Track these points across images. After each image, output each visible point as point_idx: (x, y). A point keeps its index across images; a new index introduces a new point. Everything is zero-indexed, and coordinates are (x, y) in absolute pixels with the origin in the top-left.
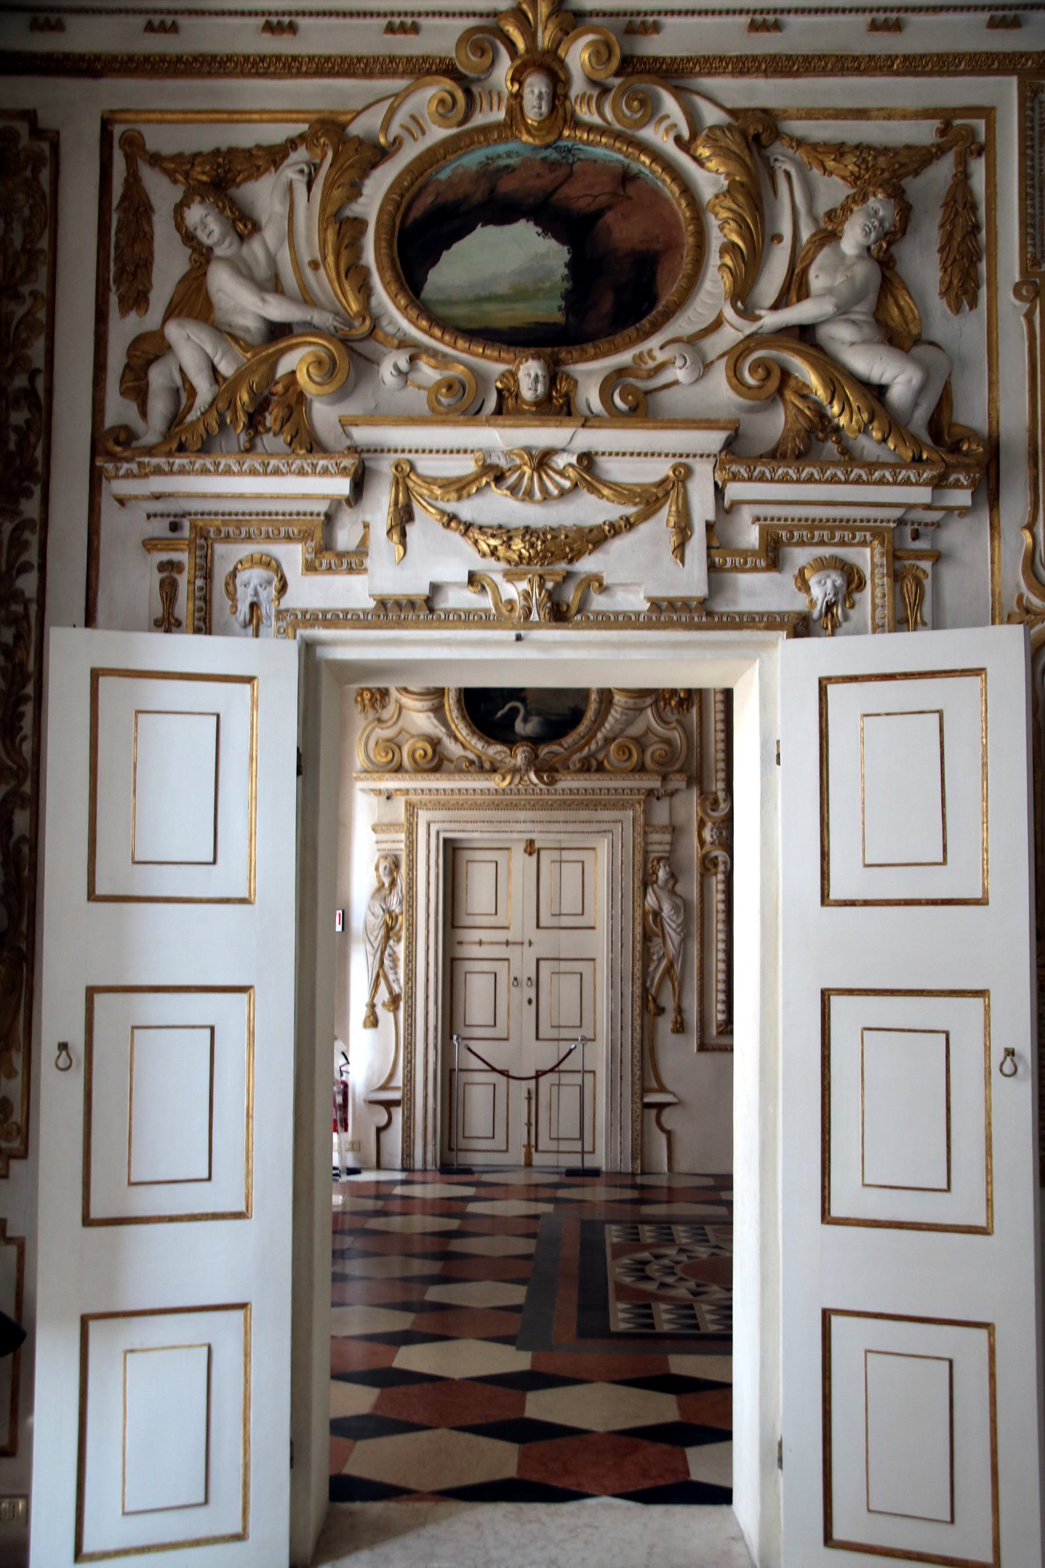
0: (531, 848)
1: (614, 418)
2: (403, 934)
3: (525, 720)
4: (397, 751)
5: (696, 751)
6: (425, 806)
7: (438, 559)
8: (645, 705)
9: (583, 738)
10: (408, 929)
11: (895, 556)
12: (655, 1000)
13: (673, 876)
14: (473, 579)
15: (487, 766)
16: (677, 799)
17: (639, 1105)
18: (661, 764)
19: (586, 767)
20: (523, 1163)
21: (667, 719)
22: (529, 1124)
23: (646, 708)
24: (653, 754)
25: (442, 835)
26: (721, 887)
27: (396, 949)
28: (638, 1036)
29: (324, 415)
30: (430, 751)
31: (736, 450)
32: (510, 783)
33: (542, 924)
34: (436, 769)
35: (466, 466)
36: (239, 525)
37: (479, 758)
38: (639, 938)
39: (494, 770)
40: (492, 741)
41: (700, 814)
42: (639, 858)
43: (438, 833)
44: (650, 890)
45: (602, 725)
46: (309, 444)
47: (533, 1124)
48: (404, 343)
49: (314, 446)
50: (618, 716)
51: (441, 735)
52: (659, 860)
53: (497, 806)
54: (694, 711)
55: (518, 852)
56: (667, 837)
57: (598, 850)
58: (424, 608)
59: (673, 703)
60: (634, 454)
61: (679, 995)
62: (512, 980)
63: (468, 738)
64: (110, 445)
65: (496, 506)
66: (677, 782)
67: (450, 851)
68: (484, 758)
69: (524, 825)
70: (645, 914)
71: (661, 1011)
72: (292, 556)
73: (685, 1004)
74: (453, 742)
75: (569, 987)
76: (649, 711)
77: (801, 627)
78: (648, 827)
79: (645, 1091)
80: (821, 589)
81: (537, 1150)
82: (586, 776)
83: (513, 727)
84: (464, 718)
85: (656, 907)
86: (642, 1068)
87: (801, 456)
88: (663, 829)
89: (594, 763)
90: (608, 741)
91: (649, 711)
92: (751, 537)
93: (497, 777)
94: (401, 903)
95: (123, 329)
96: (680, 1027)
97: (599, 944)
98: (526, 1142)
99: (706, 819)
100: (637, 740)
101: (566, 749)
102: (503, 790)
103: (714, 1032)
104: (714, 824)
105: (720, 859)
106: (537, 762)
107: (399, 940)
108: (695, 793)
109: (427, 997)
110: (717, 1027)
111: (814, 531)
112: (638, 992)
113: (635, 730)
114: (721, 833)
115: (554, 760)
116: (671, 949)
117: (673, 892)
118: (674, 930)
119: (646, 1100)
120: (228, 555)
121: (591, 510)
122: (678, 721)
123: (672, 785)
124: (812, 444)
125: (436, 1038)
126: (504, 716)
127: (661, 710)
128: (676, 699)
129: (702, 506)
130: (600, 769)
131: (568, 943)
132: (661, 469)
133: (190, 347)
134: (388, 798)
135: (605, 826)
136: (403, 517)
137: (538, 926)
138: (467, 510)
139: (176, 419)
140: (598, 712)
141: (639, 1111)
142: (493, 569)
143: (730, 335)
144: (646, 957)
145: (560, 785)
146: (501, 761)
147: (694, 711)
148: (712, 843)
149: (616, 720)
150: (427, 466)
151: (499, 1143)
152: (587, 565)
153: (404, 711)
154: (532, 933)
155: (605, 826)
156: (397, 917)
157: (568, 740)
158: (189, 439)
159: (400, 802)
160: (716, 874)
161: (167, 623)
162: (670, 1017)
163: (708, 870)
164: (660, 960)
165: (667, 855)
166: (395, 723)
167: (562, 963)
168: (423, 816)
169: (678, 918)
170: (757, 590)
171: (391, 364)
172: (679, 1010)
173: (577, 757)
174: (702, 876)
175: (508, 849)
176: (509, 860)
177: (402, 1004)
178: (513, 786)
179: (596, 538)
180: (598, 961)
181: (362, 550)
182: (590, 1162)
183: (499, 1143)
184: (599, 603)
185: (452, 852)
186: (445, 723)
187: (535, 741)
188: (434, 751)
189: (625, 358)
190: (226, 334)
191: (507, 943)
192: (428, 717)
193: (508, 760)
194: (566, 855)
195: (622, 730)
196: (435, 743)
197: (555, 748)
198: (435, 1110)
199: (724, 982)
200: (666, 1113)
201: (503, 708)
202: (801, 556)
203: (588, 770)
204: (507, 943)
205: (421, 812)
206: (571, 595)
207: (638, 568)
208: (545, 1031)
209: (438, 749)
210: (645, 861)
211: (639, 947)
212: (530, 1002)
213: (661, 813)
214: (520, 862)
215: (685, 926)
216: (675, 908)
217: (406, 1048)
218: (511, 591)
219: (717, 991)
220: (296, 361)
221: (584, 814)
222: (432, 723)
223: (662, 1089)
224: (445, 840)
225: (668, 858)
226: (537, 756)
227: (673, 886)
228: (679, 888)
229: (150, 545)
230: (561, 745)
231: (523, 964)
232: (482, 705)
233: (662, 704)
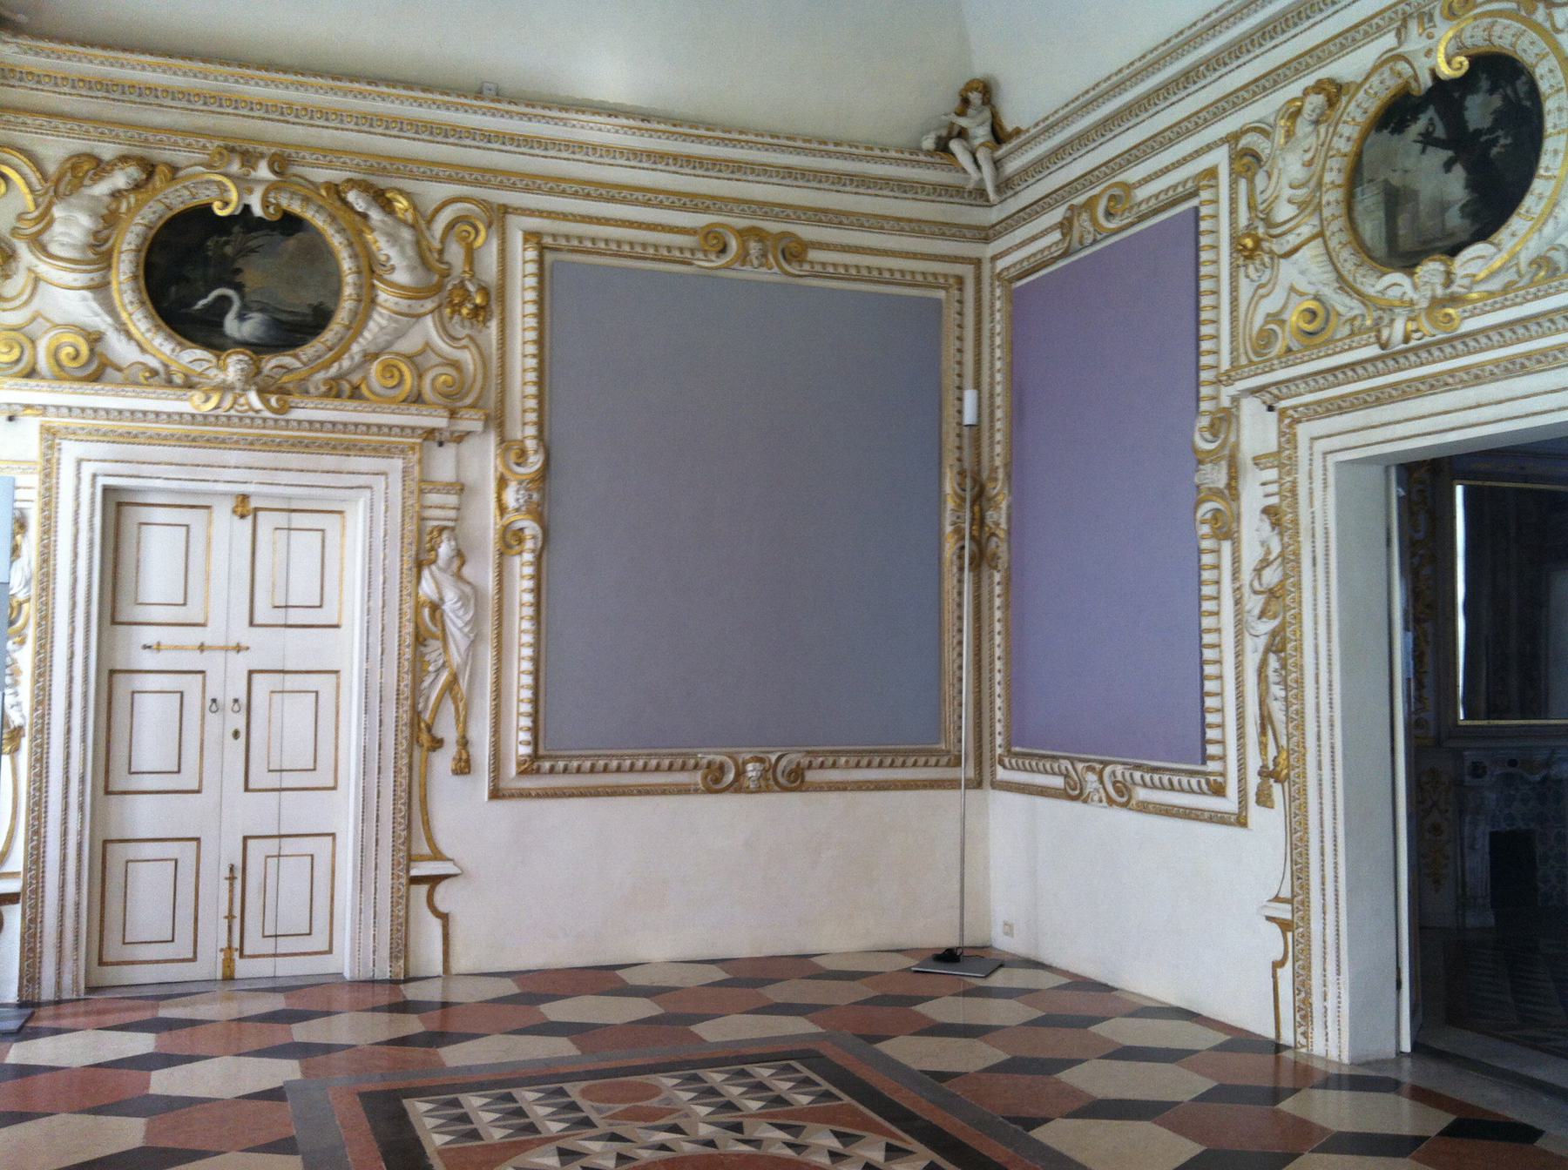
0: (243, 507)
2: (31, 633)
3: (241, 317)
4: (28, 346)
5: (494, 381)
6: (71, 433)
8: (422, 310)
9: (330, 349)
10: (39, 625)
12: (429, 728)
13: (460, 556)
15: (178, 379)
16: (468, 446)
17: (404, 881)
18: (447, 396)
19: (334, 392)
20: (219, 976)
21: (453, 333)
22: (230, 917)
23: (425, 314)
24: (434, 380)
25: (101, 481)
26: (529, 570)
27: (16, 655)
28: (405, 782)
30: (84, 350)
32: (216, 408)
33: (258, 620)
34: (96, 378)
37: (166, 366)
38: (409, 640)
39: (189, 385)
40: (188, 343)
41: (500, 469)
42: (411, 526)
43: (94, 476)
44: (426, 573)
45: (359, 333)
47: (236, 917)
50: (384, 322)
51: (103, 327)
52: (442, 530)
53: (192, 441)
54: (494, 325)
55: (223, 513)
56: (452, 500)
57: (348, 515)
59: (465, 311)
61: (463, 721)
62: (208, 703)
63: (149, 335)
66: (471, 422)
67: (112, 508)
68: (174, 367)
69: (236, 470)
70: (418, 607)
71: (437, 744)
73: (473, 734)
74: (123, 338)
75: (297, 713)
76: (429, 321)
78: (425, 485)
79: (410, 859)
81: (242, 955)
82: (337, 402)
83: (221, 325)
84: (142, 303)
85: (435, 597)
86: (409, 827)
88: (448, 488)
89: (346, 387)
90: (369, 357)
91: (429, 321)
93: (197, 396)
94: (27, 583)
96: (464, 767)
97: (348, 650)
98: (224, 945)
99: (508, 475)
100: (410, 358)
101: (305, 364)
102: (205, 416)
103: (512, 770)
104: (520, 483)
105: (528, 532)
106: (258, 379)
107: (22, 643)
108: (492, 440)
109: (69, 731)
110: (519, 764)
112: (406, 718)
113: (408, 345)
114: (530, 497)
115: (285, 379)
116: (456, 658)
117: (459, 576)
118: (460, 629)
119: (414, 873)
122: (471, 338)
123: (463, 425)
125: (82, 793)
126: (207, 308)
127: (446, 320)
128: (470, 306)
130: (355, 394)
131: (297, 648)
134: (11, 419)
135: (362, 480)
137: (251, 624)
140: (354, 314)
141: (403, 889)
144: (418, 668)
145: (296, 414)
146: (201, 374)
147: (494, 325)
148: (517, 510)
149: (382, 328)
151: (183, 948)
153: (42, 284)
155: (362, 480)
156: (20, 605)
157: (309, 351)
159: (30, 426)
160: (520, 553)
162: (449, 752)
163: (508, 546)
164: (438, 671)
165: (450, 524)
166: (26, 303)
167: (288, 676)
168: (70, 451)
169: (466, 613)
172: (464, 743)
173: (321, 376)
174: (501, 554)
175: (207, 507)
176: (210, 523)
177: (25, 743)
178: (219, 412)
180: (344, 676)
183: (183, 948)
185: (117, 507)
186: (111, 311)
187: (258, 348)
188: (92, 351)
191: (202, 648)
192: (84, 299)
193: (213, 372)
194: (299, 520)
195: (390, 344)
196: (95, 339)
197: (286, 360)
198: (78, 904)
199: (531, 701)
200: (441, 889)
201: (205, 296)
203: (338, 396)
204: (202, 648)
205: (66, 445)
208: (259, 778)
209: (99, 348)
210: (420, 532)
211: (408, 653)
212: (236, 734)
213: (444, 464)
215: (475, 623)
216: (463, 598)
217: (30, 810)
219: (519, 714)
221: (329, 461)
222: (89, 307)
223: (437, 856)
224: (107, 490)
225: (453, 529)
226: (259, 372)
227: (460, 568)
228: (467, 571)
230: (296, 357)
231: (227, 679)
232: (173, 289)
233: (448, 311)
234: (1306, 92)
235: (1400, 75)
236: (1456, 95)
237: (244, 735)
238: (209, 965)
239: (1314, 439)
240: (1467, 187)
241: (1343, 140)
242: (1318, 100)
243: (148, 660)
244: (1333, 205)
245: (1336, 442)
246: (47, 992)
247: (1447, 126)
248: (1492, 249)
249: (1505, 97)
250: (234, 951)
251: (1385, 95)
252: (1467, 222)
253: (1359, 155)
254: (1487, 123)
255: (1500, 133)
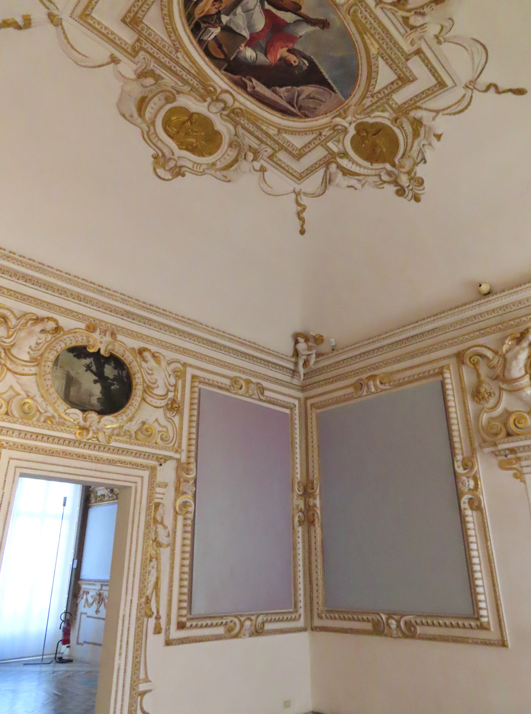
234: (49, 319)
235: (89, 341)
236: (102, 361)
239: (11, 458)
240: (101, 393)
241: (60, 347)
242: (51, 325)
244: (49, 368)
245: (25, 464)
247: (97, 369)
248: (116, 421)
249: (119, 373)
251: (79, 344)
252: (99, 405)
253: (58, 356)
254: (111, 377)
255: (115, 383)
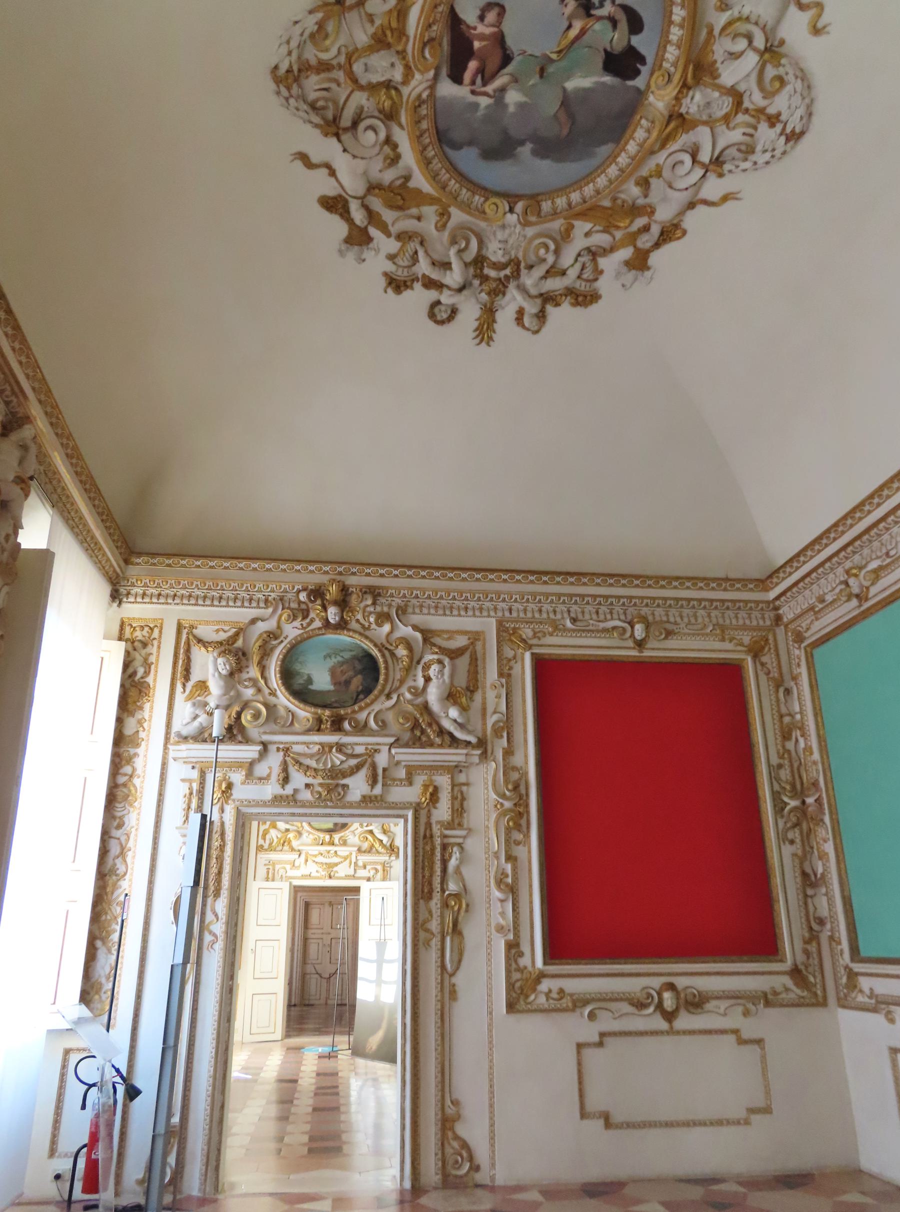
1: (341, 845)
7: (312, 868)
11: (384, 866)
14: (317, 871)
29: (295, 844)
31: (359, 850)
35: (316, 853)
36: (280, 862)
46: (293, 850)
48: (308, 831)
49: (293, 850)
55: (327, 905)
58: (309, 876)
60: (343, 851)
64: (260, 848)
65: (320, 859)
72: (288, 867)
77: (369, 879)
80: (373, 872)
87: (369, 852)
92: (360, 863)
95: (262, 828)
111: (371, 863)
120: (277, 867)
121: (336, 860)
124: (369, 851)
129: (354, 860)
132: (348, 853)
133: (273, 833)
136: (306, 861)
138: (317, 860)
139: (270, 844)
142: (320, 870)
143: (360, 830)
150: (310, 852)
152: (335, 869)
154: (330, 930)
158: (271, 848)
161: (267, 879)
168: (299, 894)
170: (361, 873)
171: (305, 835)
179: (336, 864)
181: (299, 866)
182: (344, 1002)
183: (318, 997)
184: (336, 875)
185: (307, 905)
189: (342, 834)
190: (279, 830)
202: (368, 867)
206: (332, 874)
207: (343, 870)
214: (327, 909)
218: (323, 873)
220: (291, 835)
229: (265, 865)
237: (330, 952)
238: (322, 1001)
243: (313, 936)
246: (293, 1003)
250: (327, 998)
